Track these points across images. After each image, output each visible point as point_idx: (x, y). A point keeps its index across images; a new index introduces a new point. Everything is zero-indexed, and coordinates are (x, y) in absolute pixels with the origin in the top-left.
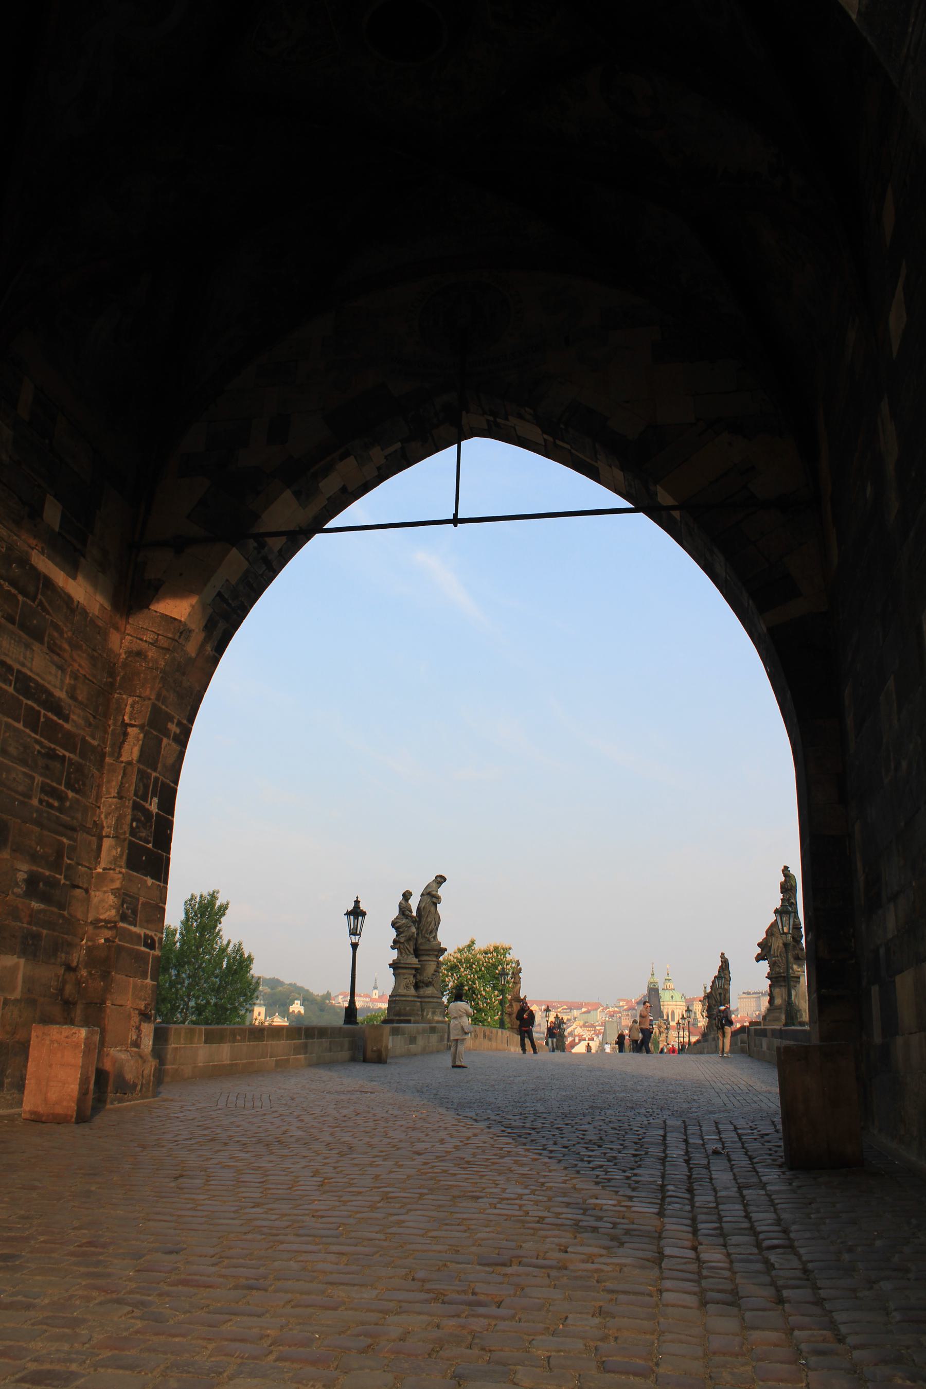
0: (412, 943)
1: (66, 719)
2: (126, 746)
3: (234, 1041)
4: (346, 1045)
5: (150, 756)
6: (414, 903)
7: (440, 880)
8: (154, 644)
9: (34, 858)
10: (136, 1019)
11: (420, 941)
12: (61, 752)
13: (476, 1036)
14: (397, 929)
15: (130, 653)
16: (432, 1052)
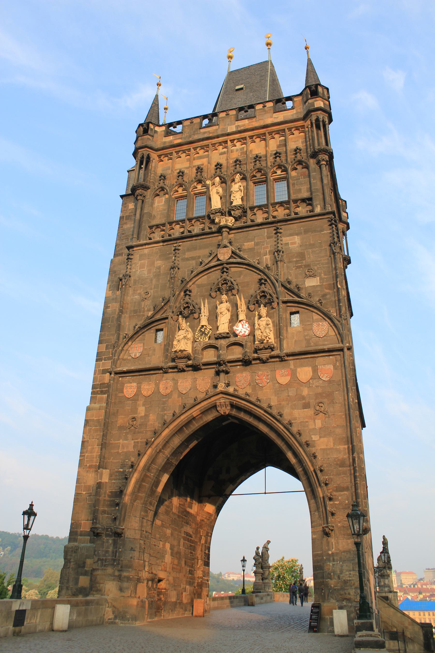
0: (260, 565)
1: (192, 537)
2: (202, 540)
3: (218, 600)
4: (243, 601)
5: (206, 542)
6: (260, 551)
7: (269, 542)
8: (206, 518)
9: (190, 566)
10: (206, 597)
11: (263, 564)
12: (192, 544)
13: (284, 596)
14: (255, 560)
15: (201, 520)
16: (268, 602)
